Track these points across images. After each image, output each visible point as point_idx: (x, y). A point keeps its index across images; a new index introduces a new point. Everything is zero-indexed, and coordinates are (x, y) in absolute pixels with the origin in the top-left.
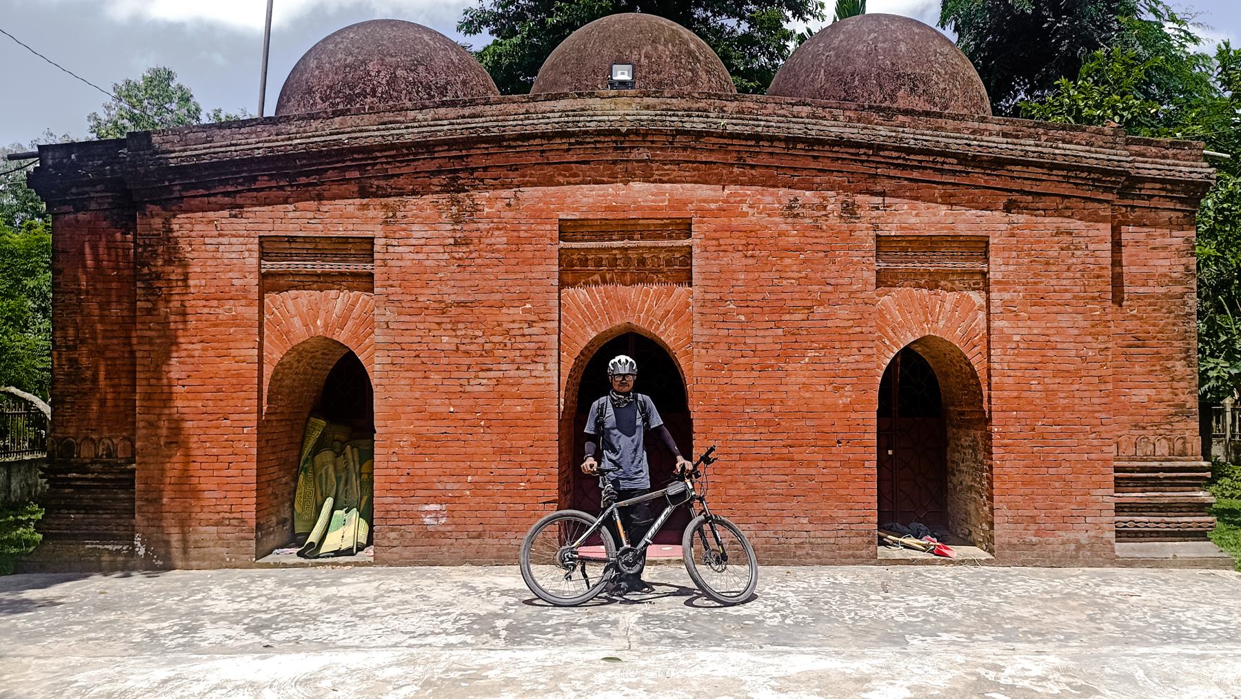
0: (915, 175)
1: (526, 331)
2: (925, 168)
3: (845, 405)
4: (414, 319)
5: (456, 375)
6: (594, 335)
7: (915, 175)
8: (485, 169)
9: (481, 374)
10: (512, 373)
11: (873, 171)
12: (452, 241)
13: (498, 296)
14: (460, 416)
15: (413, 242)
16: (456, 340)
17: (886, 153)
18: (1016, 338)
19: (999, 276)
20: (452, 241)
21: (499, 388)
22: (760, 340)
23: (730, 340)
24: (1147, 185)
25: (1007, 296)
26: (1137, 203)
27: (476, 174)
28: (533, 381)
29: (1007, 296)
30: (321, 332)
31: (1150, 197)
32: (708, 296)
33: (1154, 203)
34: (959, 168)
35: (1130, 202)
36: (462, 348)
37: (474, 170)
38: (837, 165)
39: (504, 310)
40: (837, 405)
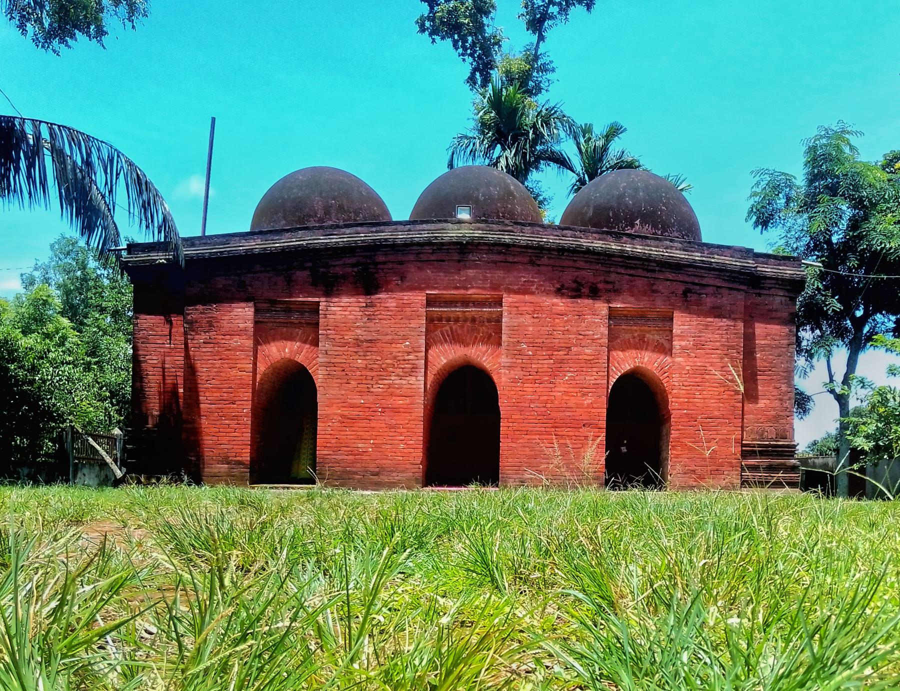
0: (632, 272)
1: (406, 358)
2: (638, 268)
3: (588, 404)
4: (342, 349)
5: (364, 382)
6: (445, 361)
7: (632, 272)
8: (384, 263)
9: (380, 382)
10: (398, 382)
11: (608, 269)
12: (364, 305)
13: (390, 337)
14: (367, 405)
15: (342, 304)
16: (365, 362)
17: (616, 259)
18: (688, 368)
19: (679, 332)
20: (364, 305)
21: (389, 390)
22: (540, 366)
23: (523, 365)
24: (768, 281)
25: (683, 343)
26: (762, 292)
27: (379, 266)
28: (409, 386)
29: (683, 343)
30: (288, 356)
31: (770, 288)
32: (512, 340)
33: (772, 291)
34: (657, 269)
35: (758, 291)
36: (370, 366)
37: (380, 263)
38: (587, 266)
39: (393, 345)
40: (583, 404)
